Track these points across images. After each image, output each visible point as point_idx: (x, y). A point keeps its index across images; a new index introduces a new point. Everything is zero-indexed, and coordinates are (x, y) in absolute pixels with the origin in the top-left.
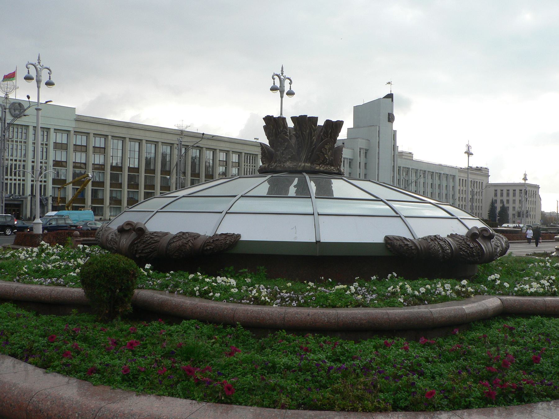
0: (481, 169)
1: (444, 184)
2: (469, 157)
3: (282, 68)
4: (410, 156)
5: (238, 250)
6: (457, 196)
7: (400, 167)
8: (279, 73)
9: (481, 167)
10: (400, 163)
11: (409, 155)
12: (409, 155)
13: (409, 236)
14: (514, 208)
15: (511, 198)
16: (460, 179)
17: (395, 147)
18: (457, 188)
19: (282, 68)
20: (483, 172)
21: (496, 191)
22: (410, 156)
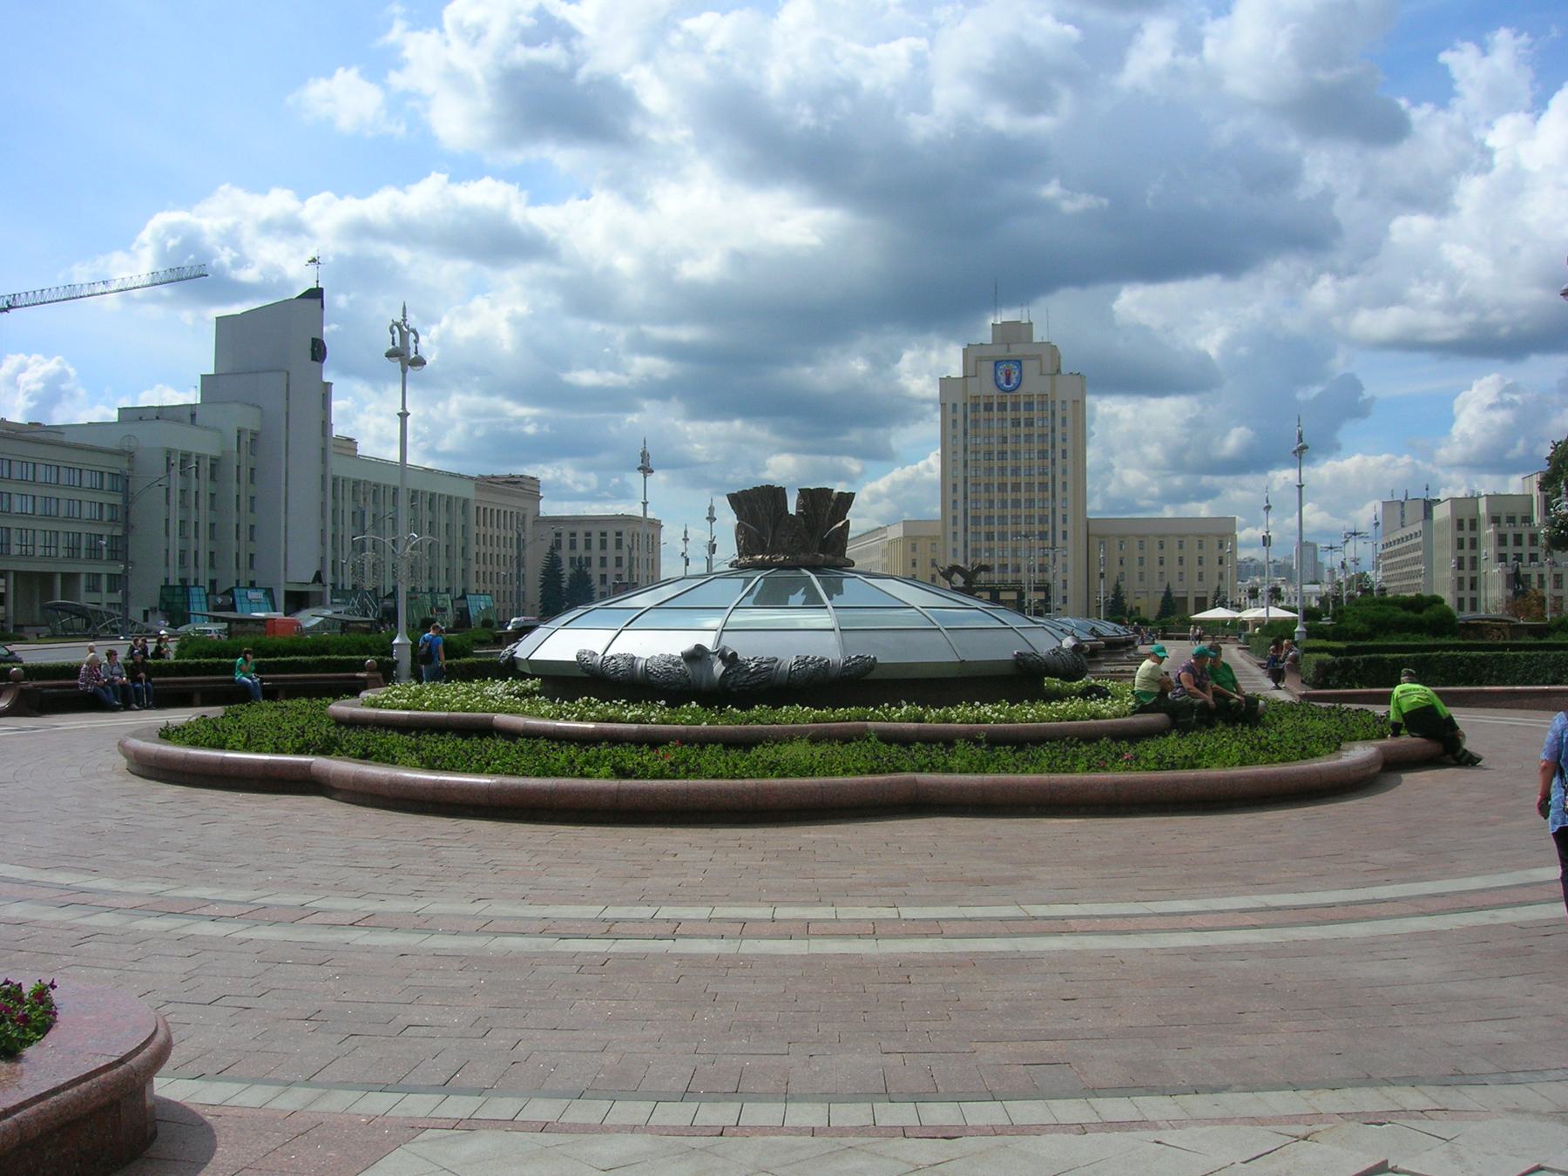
0: (521, 480)
1: (443, 520)
2: (645, 477)
3: (404, 309)
4: (350, 448)
5: (874, 675)
6: (473, 550)
7: (335, 479)
8: (399, 319)
9: (521, 476)
10: (338, 467)
11: (347, 444)
12: (347, 444)
13: (1030, 651)
14: (603, 578)
15: (596, 553)
16: (478, 508)
17: (326, 425)
18: (474, 529)
19: (404, 309)
20: (527, 487)
21: (559, 535)
22: (350, 448)
